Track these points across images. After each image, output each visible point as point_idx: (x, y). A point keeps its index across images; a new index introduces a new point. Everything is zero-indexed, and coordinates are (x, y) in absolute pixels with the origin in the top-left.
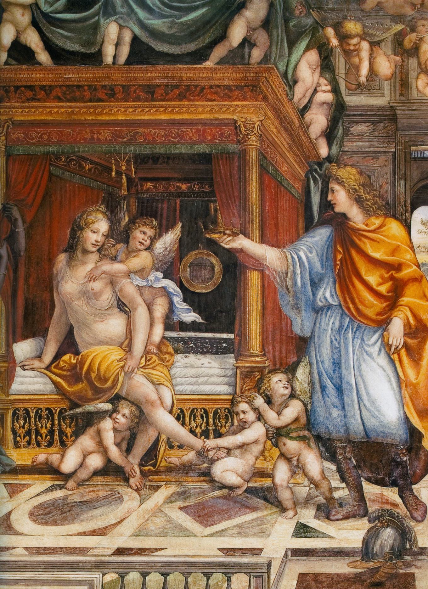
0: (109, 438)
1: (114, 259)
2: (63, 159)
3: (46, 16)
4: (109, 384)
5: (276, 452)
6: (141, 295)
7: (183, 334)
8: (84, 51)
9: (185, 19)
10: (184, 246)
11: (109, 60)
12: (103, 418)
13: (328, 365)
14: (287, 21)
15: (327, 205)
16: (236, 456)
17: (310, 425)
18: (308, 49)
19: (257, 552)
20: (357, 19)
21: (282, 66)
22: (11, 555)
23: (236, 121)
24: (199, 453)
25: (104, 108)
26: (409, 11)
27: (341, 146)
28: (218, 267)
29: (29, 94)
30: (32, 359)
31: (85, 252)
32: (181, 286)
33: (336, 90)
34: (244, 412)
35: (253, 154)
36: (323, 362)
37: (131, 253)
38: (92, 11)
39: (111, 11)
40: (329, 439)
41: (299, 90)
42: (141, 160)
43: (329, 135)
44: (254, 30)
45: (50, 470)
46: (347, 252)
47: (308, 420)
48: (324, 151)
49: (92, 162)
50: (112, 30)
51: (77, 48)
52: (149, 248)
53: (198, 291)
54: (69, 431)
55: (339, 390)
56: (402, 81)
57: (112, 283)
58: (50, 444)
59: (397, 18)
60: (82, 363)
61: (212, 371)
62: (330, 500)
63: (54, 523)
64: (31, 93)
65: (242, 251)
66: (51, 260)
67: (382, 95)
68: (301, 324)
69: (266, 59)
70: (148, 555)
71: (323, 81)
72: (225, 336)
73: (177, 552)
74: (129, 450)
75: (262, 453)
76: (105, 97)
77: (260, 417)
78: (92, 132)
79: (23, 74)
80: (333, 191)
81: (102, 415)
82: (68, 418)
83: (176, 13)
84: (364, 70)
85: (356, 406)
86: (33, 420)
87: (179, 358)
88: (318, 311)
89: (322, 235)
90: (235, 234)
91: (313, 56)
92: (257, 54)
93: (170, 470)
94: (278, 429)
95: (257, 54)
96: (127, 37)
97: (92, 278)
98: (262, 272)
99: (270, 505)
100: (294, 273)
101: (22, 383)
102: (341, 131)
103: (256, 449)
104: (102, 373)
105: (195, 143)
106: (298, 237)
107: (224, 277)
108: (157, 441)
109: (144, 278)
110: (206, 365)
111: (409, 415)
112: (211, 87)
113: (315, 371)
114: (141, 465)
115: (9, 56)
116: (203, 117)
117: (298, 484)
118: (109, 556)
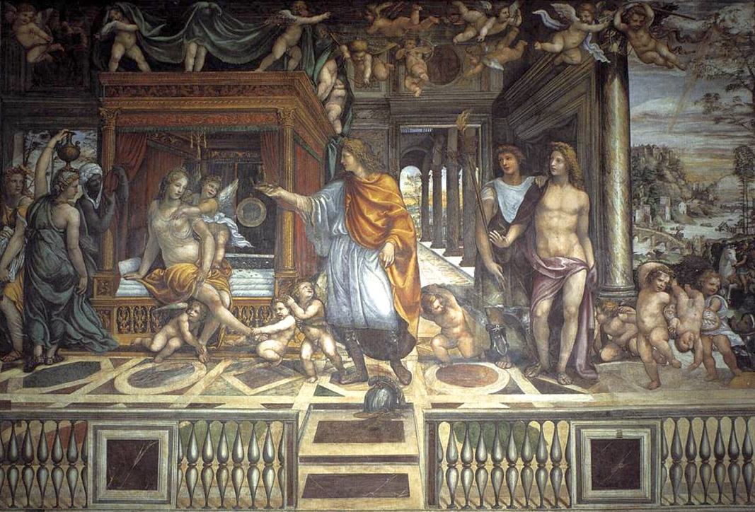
0: (186, 326)
1: (191, 204)
2: (157, 135)
3: (145, 38)
4: (186, 289)
5: (302, 337)
6: (209, 229)
7: (238, 255)
8: (173, 62)
9: (243, 40)
10: (239, 197)
11: (190, 68)
12: (182, 313)
13: (339, 275)
14: (314, 41)
15: (340, 165)
16: (274, 339)
17: (326, 318)
18: (328, 59)
19: (290, 406)
20: (364, 40)
21: (310, 72)
22: (114, 409)
23: (277, 109)
24: (248, 337)
25: (185, 101)
26: (400, 34)
27: (350, 126)
28: (263, 209)
29: (134, 91)
30: (130, 272)
31: (171, 199)
32: (237, 222)
33: (347, 88)
34: (280, 309)
35: (289, 131)
36: (336, 274)
37: (203, 200)
38: (178, 35)
39: (191, 35)
40: (340, 327)
41: (322, 88)
42: (211, 137)
43: (343, 118)
44: (291, 47)
45: (144, 349)
46: (354, 199)
47: (326, 314)
48: (339, 130)
49: (176, 137)
50: (193, 48)
51: (168, 60)
52: (215, 197)
53: (249, 226)
54: (157, 322)
55: (348, 293)
56: (395, 83)
57: (189, 220)
58: (144, 331)
59: (390, 39)
60: (167, 275)
61: (257, 281)
62: (341, 369)
63: (146, 386)
64: (135, 91)
65: (280, 198)
66: (147, 204)
67: (380, 91)
68: (321, 247)
69: (298, 68)
70: (212, 408)
71: (339, 82)
72: (267, 256)
73: (235, 407)
74: (199, 336)
75: (293, 336)
76: (187, 94)
77: (292, 312)
78: (177, 117)
79: (133, 79)
80: (344, 156)
81: (182, 311)
82: (158, 310)
83: (237, 36)
84: (368, 75)
85: (360, 305)
86: (132, 314)
87: (235, 271)
88: (331, 238)
89: (337, 186)
90: (275, 187)
91: (332, 65)
92: (293, 64)
93: (228, 349)
94: (304, 320)
95: (293, 64)
96: (203, 54)
97: (175, 217)
98: (294, 214)
99: (297, 374)
100: (317, 213)
101: (125, 289)
102: (351, 116)
103: (289, 334)
104: (181, 280)
105: (249, 125)
106: (320, 188)
107: (267, 217)
108: (219, 328)
109: (212, 217)
110: (254, 276)
111: (398, 310)
112: (260, 86)
113: (331, 280)
114: (207, 346)
115: (119, 65)
116: (254, 107)
117: (318, 359)
118: (187, 408)
